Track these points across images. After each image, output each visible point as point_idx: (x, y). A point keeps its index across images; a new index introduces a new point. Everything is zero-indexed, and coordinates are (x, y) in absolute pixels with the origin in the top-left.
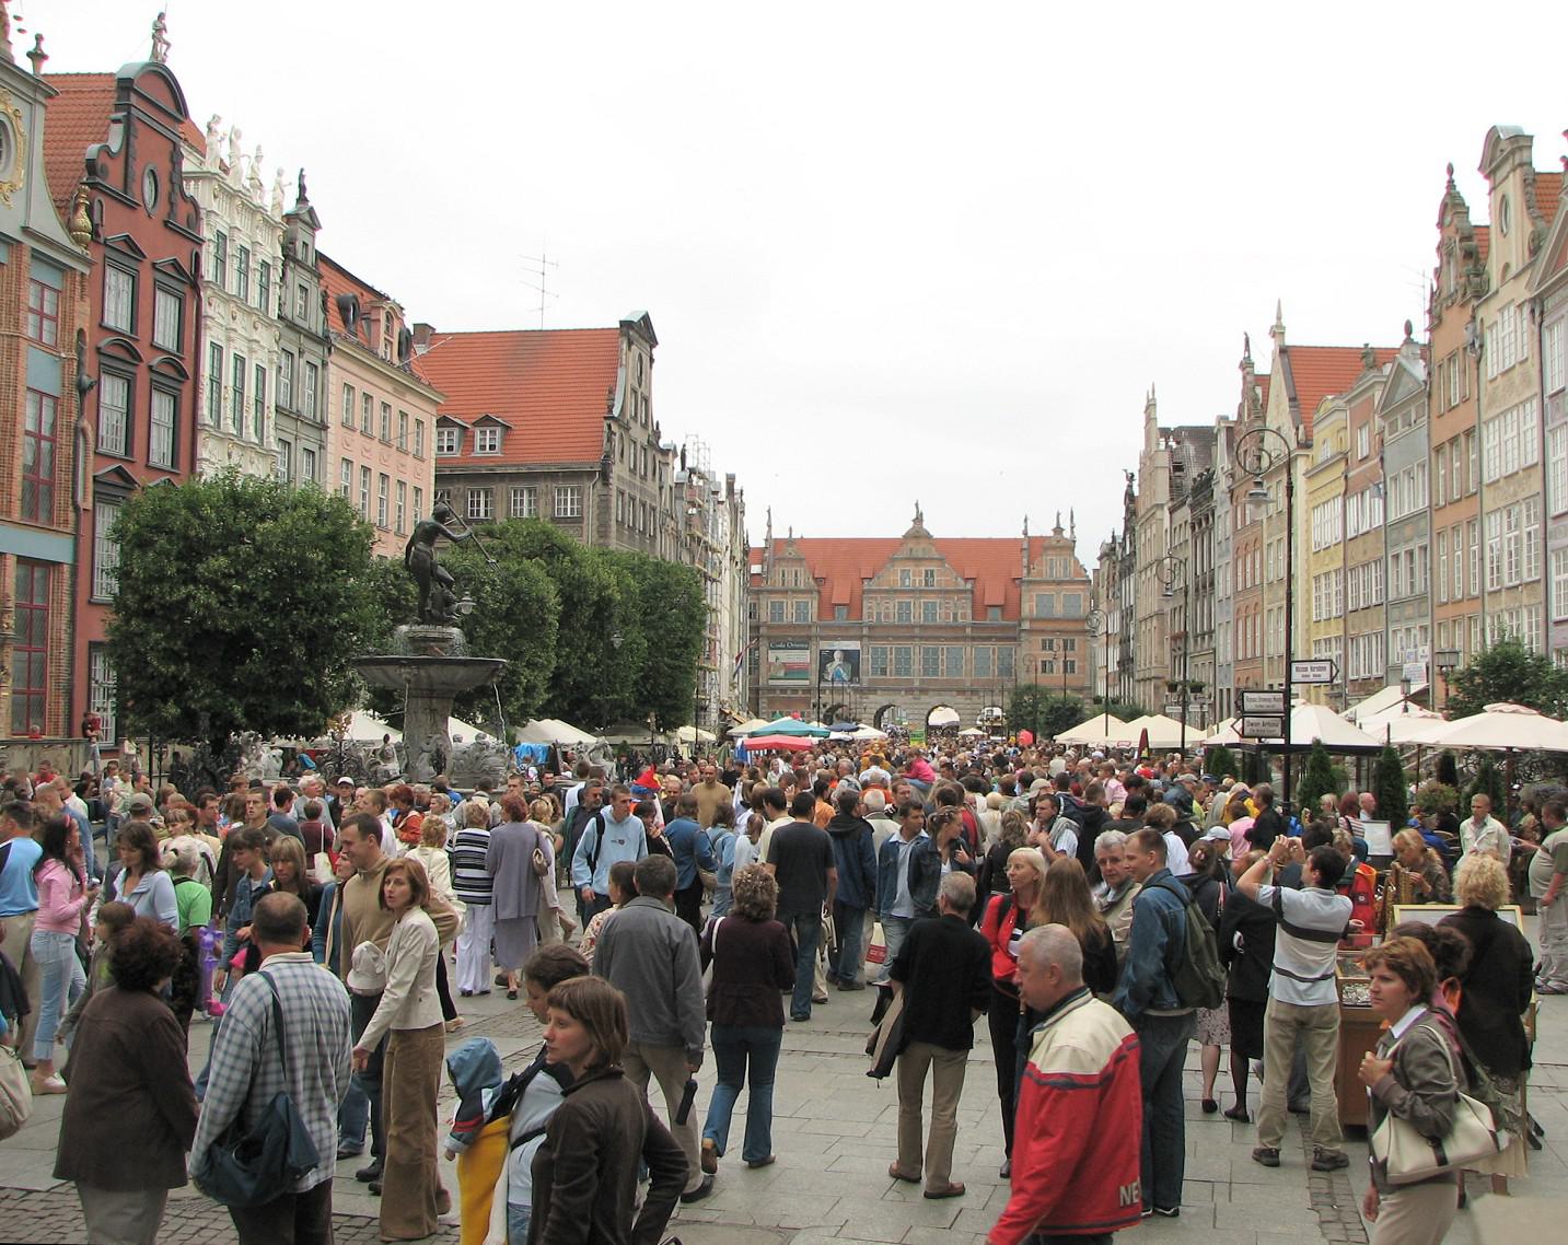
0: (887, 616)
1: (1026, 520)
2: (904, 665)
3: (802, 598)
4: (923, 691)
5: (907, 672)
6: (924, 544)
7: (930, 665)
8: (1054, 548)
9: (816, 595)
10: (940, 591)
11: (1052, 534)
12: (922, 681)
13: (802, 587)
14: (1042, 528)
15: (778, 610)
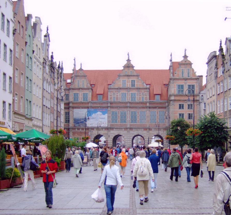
0: (117, 98)
1: (171, 55)
2: (123, 119)
3: (86, 92)
4: (131, 129)
5: (125, 122)
6: (131, 70)
7: (134, 119)
8: (184, 64)
9: (90, 90)
10: (137, 88)
11: (182, 59)
12: (131, 125)
13: (85, 87)
14: (178, 58)
15: (76, 96)
